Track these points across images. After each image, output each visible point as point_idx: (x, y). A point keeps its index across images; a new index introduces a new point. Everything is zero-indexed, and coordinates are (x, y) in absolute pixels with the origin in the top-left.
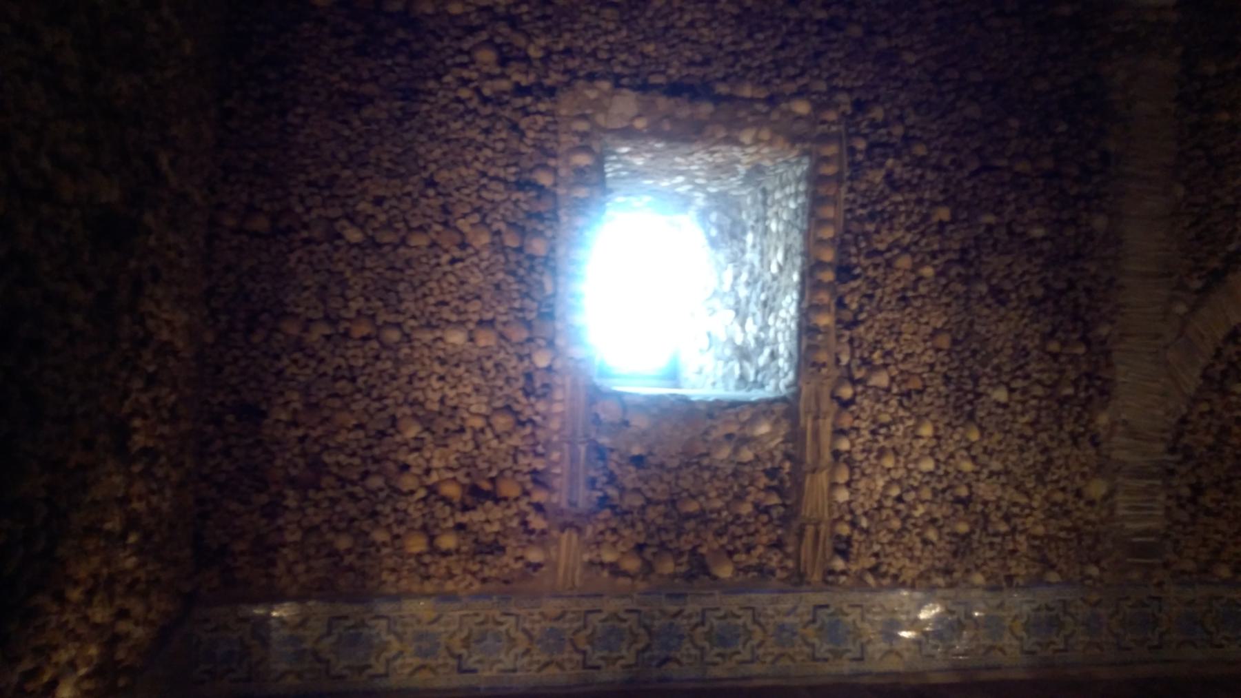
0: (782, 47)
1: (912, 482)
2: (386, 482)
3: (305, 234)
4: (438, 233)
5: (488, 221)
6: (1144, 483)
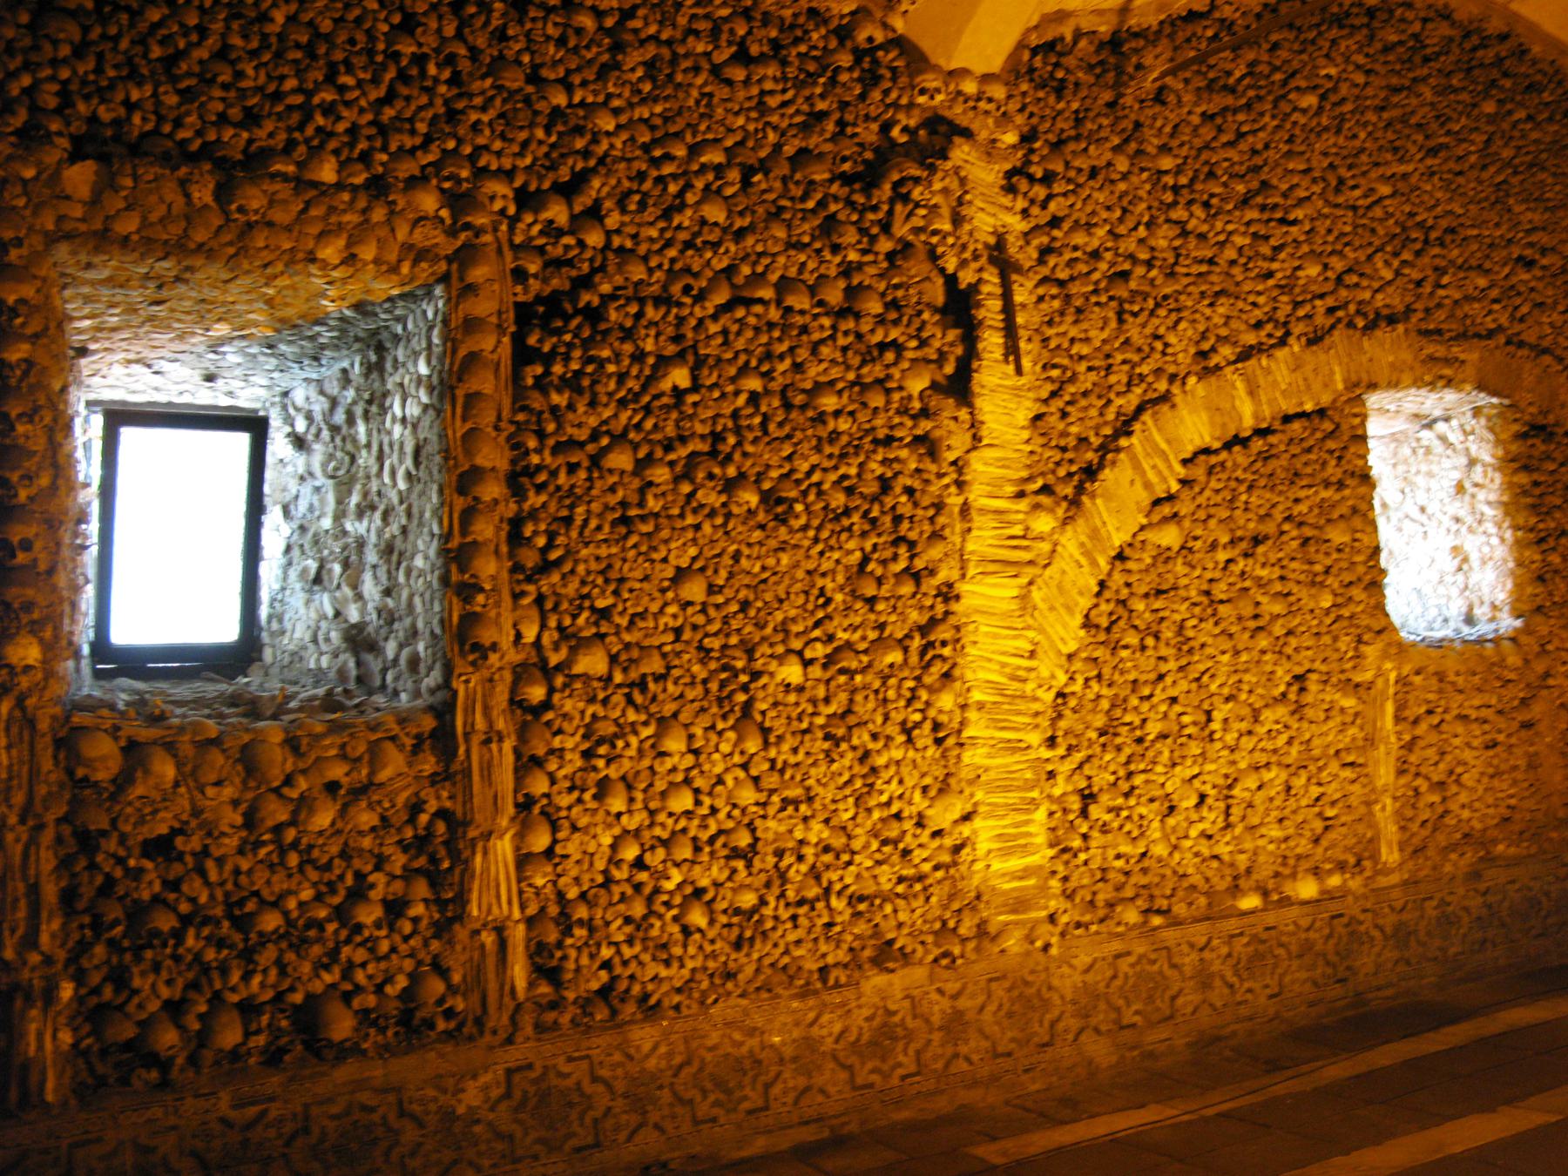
0: (389, 99)
1: (658, 831)
6: (1013, 798)
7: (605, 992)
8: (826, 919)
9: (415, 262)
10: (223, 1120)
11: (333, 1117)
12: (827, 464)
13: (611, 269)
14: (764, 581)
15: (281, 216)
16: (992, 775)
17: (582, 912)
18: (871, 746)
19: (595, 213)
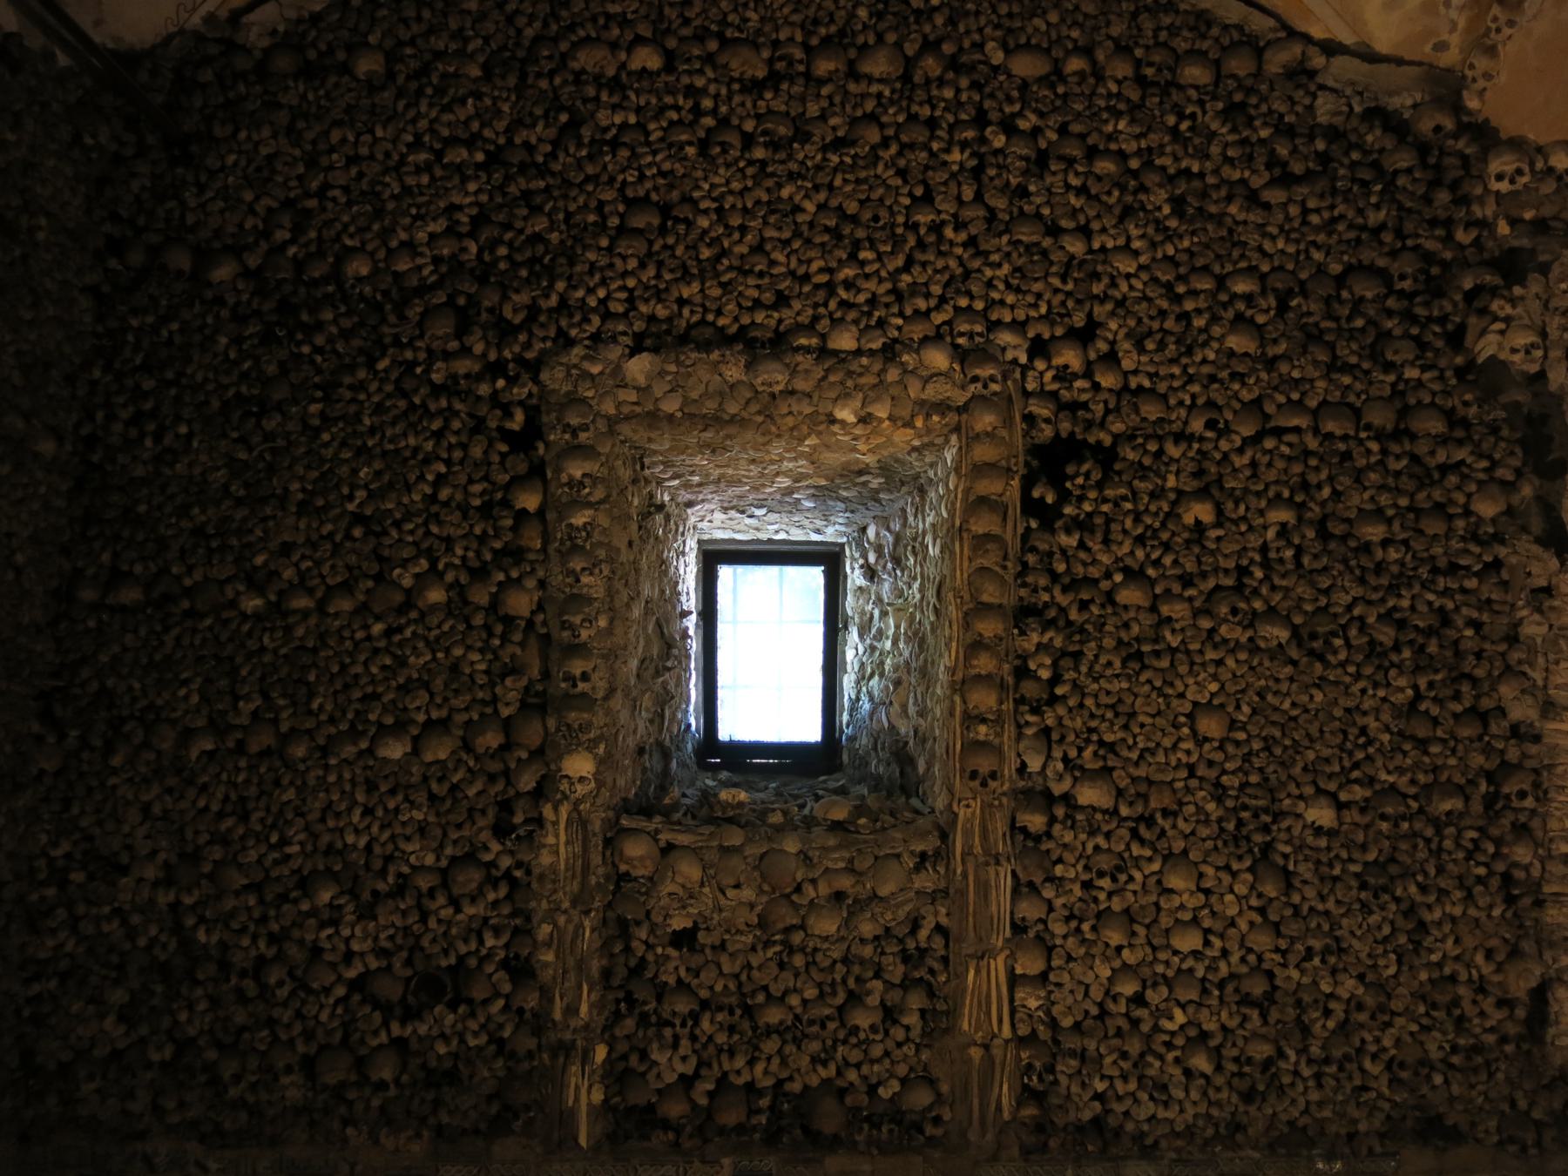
1: (1160, 969)
2: (291, 974)
3: (186, 604)
4: (368, 591)
5: (441, 566)
7: (1097, 1122)
8: (1358, 1082)
9: (928, 416)
12: (1375, 596)
13: (1125, 410)
14: (1295, 719)
15: (800, 384)
17: (1072, 1042)
18: (1419, 898)
19: (1111, 358)
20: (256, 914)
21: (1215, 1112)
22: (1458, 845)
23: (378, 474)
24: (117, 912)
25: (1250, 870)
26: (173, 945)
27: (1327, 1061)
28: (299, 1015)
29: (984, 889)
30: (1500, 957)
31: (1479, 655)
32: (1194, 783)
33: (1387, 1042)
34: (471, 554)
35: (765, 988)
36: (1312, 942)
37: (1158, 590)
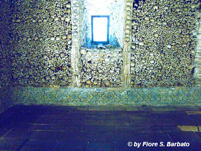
1: (149, 65)
3: (26, 22)
5: (58, 15)
7: (140, 84)
10: (95, 92)
11: (107, 93)
12: (177, 19)
16: (199, 62)
17: (138, 74)
20: (37, 60)
21: (154, 82)
22: (185, 51)
23: (49, 3)
24: (21, 60)
25: (160, 53)
26: (28, 64)
27: (168, 76)
28: (43, 72)
29: (127, 56)
30: (189, 64)
31: (190, 27)
32: (154, 42)
33: (175, 74)
34: (61, 14)
35: (100, 68)
36: (167, 62)
37: (150, 18)
